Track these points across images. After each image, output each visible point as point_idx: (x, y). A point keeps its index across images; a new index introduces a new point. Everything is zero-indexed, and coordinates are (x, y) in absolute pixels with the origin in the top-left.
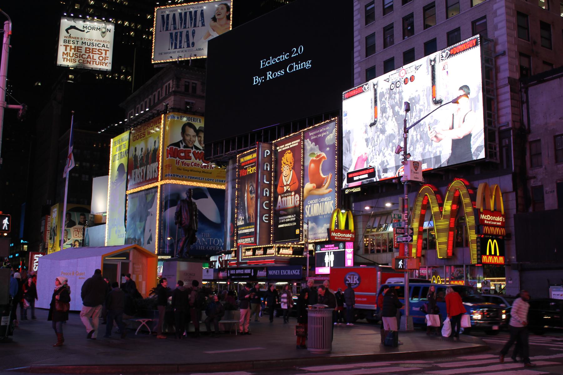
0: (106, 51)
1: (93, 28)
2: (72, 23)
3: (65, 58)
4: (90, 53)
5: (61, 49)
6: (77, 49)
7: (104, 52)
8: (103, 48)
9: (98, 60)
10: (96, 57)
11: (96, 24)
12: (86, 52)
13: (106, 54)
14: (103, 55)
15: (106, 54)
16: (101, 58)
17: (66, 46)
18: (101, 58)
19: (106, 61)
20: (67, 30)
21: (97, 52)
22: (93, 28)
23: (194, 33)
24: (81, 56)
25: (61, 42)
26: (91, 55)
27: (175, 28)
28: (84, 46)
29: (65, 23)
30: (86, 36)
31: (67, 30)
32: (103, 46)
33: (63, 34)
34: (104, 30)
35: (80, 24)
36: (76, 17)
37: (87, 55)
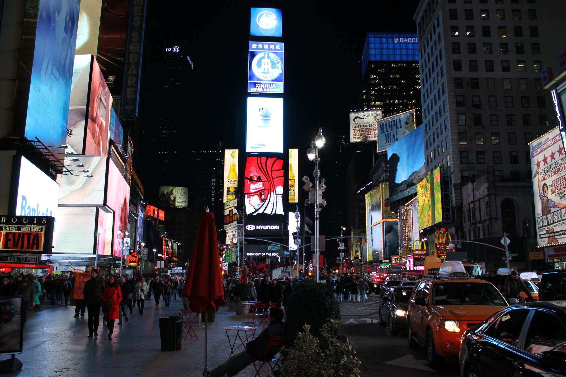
2: (356, 115)
3: (355, 138)
5: (352, 132)
6: (361, 130)
9: (374, 135)
10: (373, 133)
11: (370, 113)
17: (354, 130)
20: (354, 120)
22: (369, 116)
23: (397, 133)
24: (364, 134)
25: (351, 128)
27: (387, 131)
28: (365, 128)
29: (352, 116)
30: (365, 121)
31: (354, 120)
33: (352, 123)
35: (361, 114)
36: (358, 111)
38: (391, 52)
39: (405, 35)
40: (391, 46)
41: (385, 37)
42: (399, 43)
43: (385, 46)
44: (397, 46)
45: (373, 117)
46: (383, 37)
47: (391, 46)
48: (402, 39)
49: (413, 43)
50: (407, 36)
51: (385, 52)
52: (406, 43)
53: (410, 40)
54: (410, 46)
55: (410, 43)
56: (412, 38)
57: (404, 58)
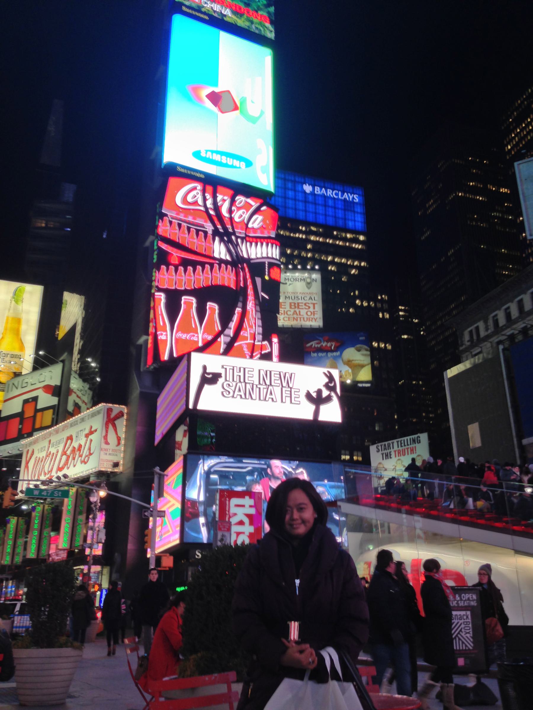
0: (314, 304)
1: (296, 280)
4: (295, 307)
7: (311, 306)
8: (310, 301)
9: (305, 316)
10: (303, 312)
12: (291, 308)
13: (314, 308)
14: (311, 309)
15: (314, 308)
16: (309, 313)
18: (309, 313)
19: (316, 316)
21: (304, 307)
22: (296, 280)
26: (297, 311)
32: (311, 298)
34: (309, 280)
37: (292, 311)
38: (301, 206)
39: (322, 184)
40: (300, 196)
41: (292, 181)
42: (313, 193)
43: (290, 194)
44: (310, 198)
45: (303, 284)
46: (288, 180)
47: (300, 196)
48: (317, 189)
49: (334, 198)
50: (326, 185)
51: (290, 203)
52: (324, 196)
53: (330, 193)
54: (330, 203)
55: (329, 197)
56: (333, 190)
57: (321, 219)
